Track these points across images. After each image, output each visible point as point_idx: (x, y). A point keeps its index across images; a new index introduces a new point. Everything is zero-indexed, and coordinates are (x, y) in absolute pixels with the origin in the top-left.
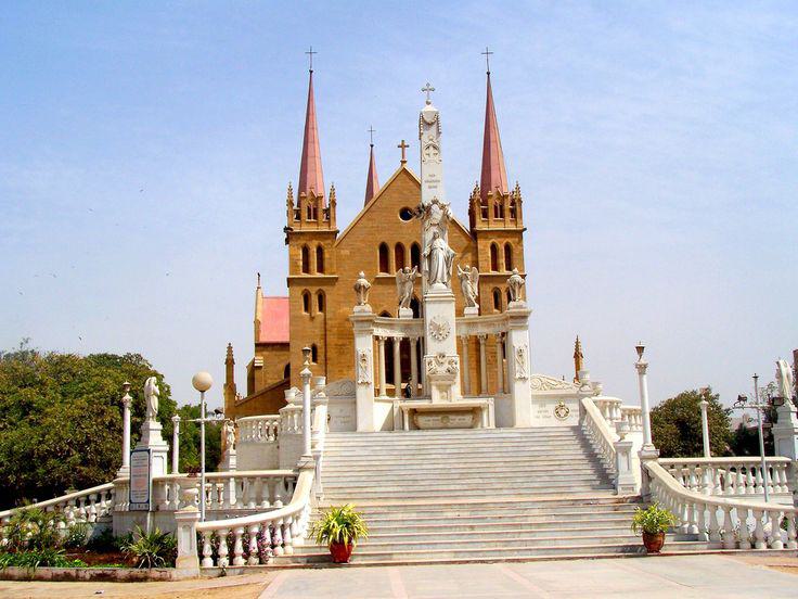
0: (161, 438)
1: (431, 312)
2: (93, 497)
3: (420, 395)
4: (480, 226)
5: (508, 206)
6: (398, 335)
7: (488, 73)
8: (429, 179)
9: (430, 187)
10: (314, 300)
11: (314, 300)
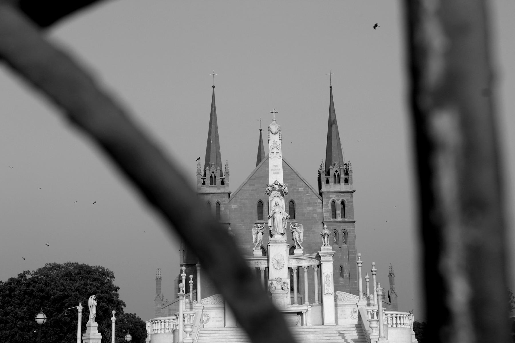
0: (97, 331)
1: (273, 251)
5: (342, 176)
7: (331, 87)
9: (274, 173)
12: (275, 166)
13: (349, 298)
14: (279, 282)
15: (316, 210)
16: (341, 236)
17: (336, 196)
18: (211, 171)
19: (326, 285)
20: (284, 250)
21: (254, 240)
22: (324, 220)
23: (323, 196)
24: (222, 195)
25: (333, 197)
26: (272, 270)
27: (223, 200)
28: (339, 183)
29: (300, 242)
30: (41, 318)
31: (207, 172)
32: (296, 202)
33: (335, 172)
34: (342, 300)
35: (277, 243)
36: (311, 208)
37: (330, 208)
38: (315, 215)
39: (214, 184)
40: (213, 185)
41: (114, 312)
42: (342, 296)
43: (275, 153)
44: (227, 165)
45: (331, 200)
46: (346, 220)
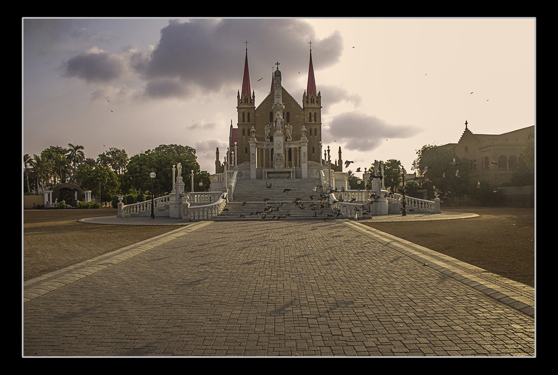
0: (182, 182)
1: (276, 139)
2: (164, 199)
4: (306, 106)
5: (315, 99)
6: (265, 147)
8: (277, 95)
9: (277, 98)
12: (277, 94)
15: (301, 117)
16: (313, 132)
18: (245, 96)
19: (303, 157)
21: (266, 133)
22: (305, 123)
23: (305, 110)
24: (251, 109)
25: (310, 110)
26: (275, 149)
27: (252, 111)
28: (313, 103)
30: (153, 175)
31: (243, 96)
32: (290, 113)
35: (279, 135)
36: (299, 116)
37: (309, 116)
38: (300, 120)
41: (192, 171)
43: (278, 87)
44: (254, 92)
45: (309, 112)
46: (317, 123)
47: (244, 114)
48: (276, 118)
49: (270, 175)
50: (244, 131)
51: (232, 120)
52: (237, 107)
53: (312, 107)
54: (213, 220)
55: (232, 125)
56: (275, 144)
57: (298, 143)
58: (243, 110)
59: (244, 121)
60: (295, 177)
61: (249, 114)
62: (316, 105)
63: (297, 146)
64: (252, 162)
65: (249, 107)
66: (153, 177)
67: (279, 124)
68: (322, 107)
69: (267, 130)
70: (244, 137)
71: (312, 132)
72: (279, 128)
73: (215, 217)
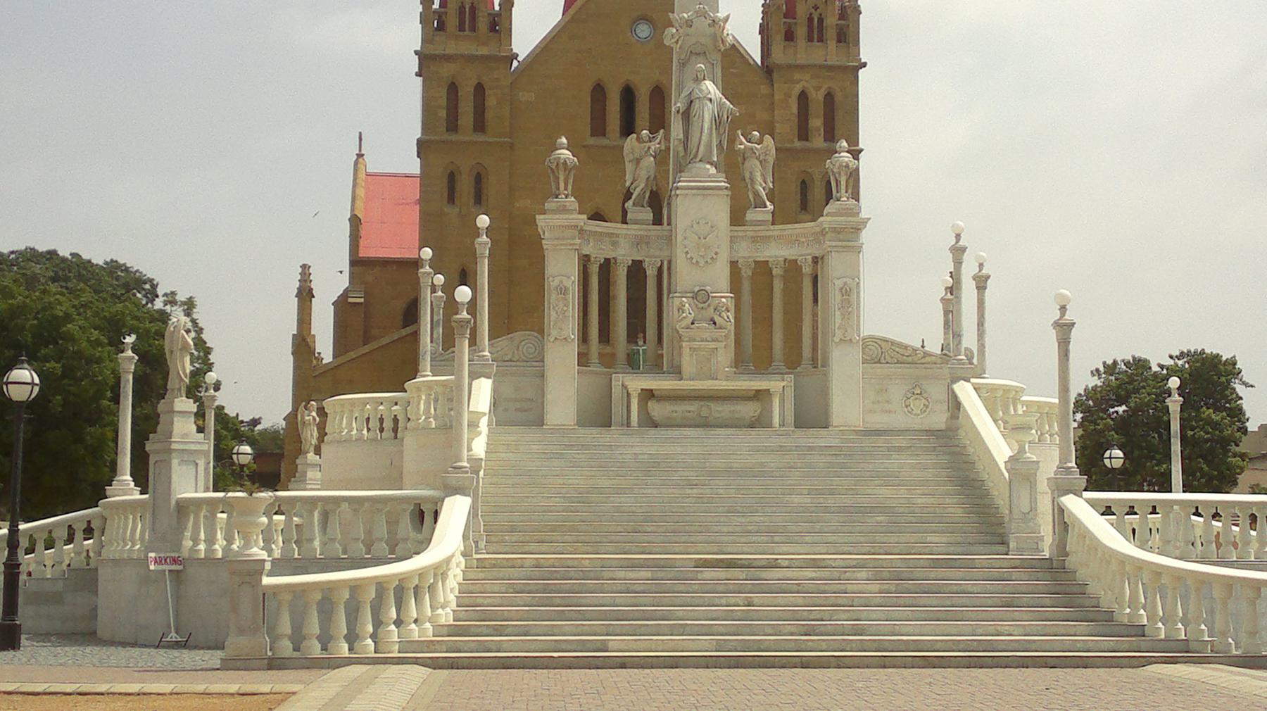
3: (656, 366)
4: (778, 56)
10: (465, 185)
11: (465, 185)
13: (903, 355)
14: (704, 303)
17: (812, 77)
19: (838, 313)
20: (720, 210)
23: (775, 75)
25: (804, 81)
26: (681, 265)
29: (764, 189)
33: (813, 11)
34: (882, 358)
37: (795, 110)
39: (470, 30)
40: (467, 33)
42: (881, 348)
47: (453, 89)
48: (685, 93)
49: (656, 409)
50: (452, 178)
51: (360, 133)
52: (416, 52)
53: (811, 62)
54: (416, 661)
55: (360, 156)
56: (680, 238)
57: (804, 235)
58: (447, 70)
59: (453, 125)
60: (790, 418)
61: (480, 90)
62: (830, 53)
63: (801, 253)
64: (554, 333)
65: (484, 51)
66: (24, 399)
67: (706, 126)
68: (864, 65)
69: (638, 161)
70: (452, 211)
71: (809, 197)
72: (702, 148)
73: (429, 646)
